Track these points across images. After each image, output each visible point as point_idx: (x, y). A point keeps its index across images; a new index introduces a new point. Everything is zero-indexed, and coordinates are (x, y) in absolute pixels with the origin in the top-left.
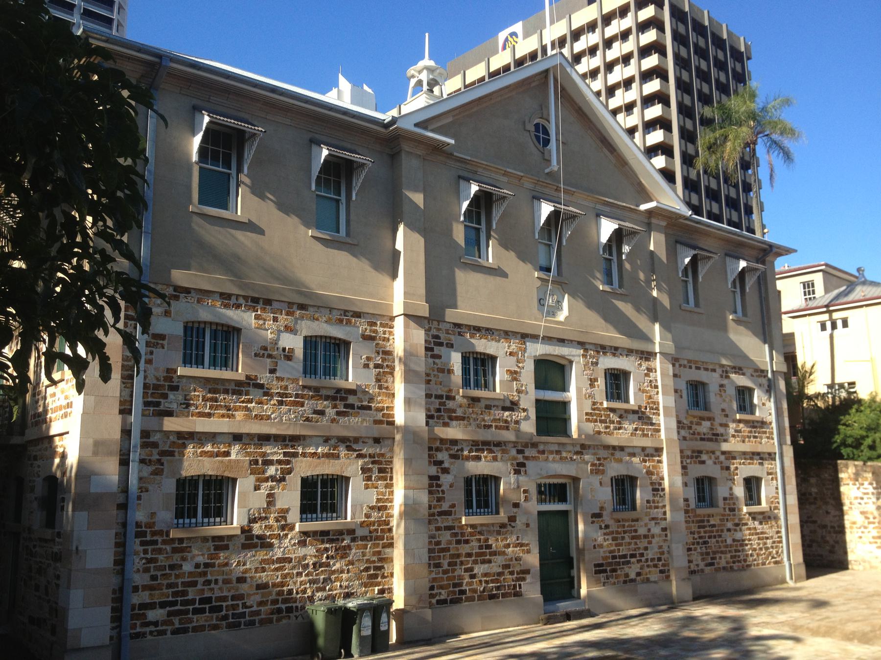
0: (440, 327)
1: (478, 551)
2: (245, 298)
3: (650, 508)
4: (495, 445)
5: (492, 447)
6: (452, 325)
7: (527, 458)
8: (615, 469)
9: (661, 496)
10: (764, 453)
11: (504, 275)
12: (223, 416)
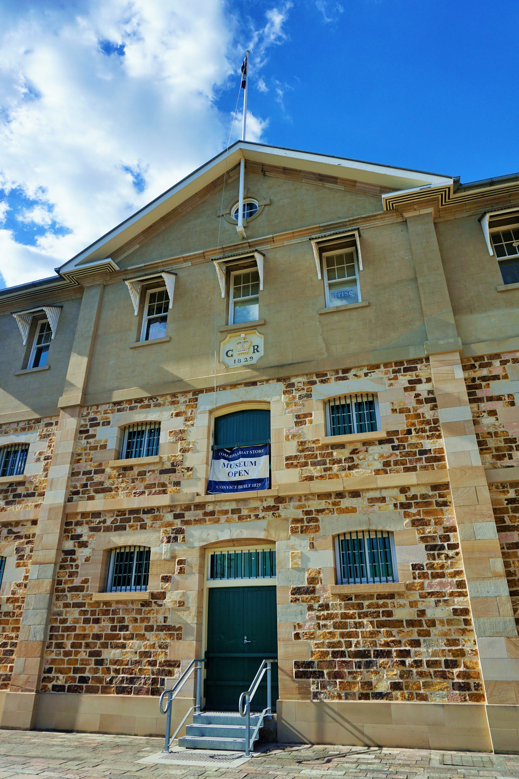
1: (110, 632)
3: (424, 576)
4: (145, 512)
5: (142, 516)
9: (447, 557)
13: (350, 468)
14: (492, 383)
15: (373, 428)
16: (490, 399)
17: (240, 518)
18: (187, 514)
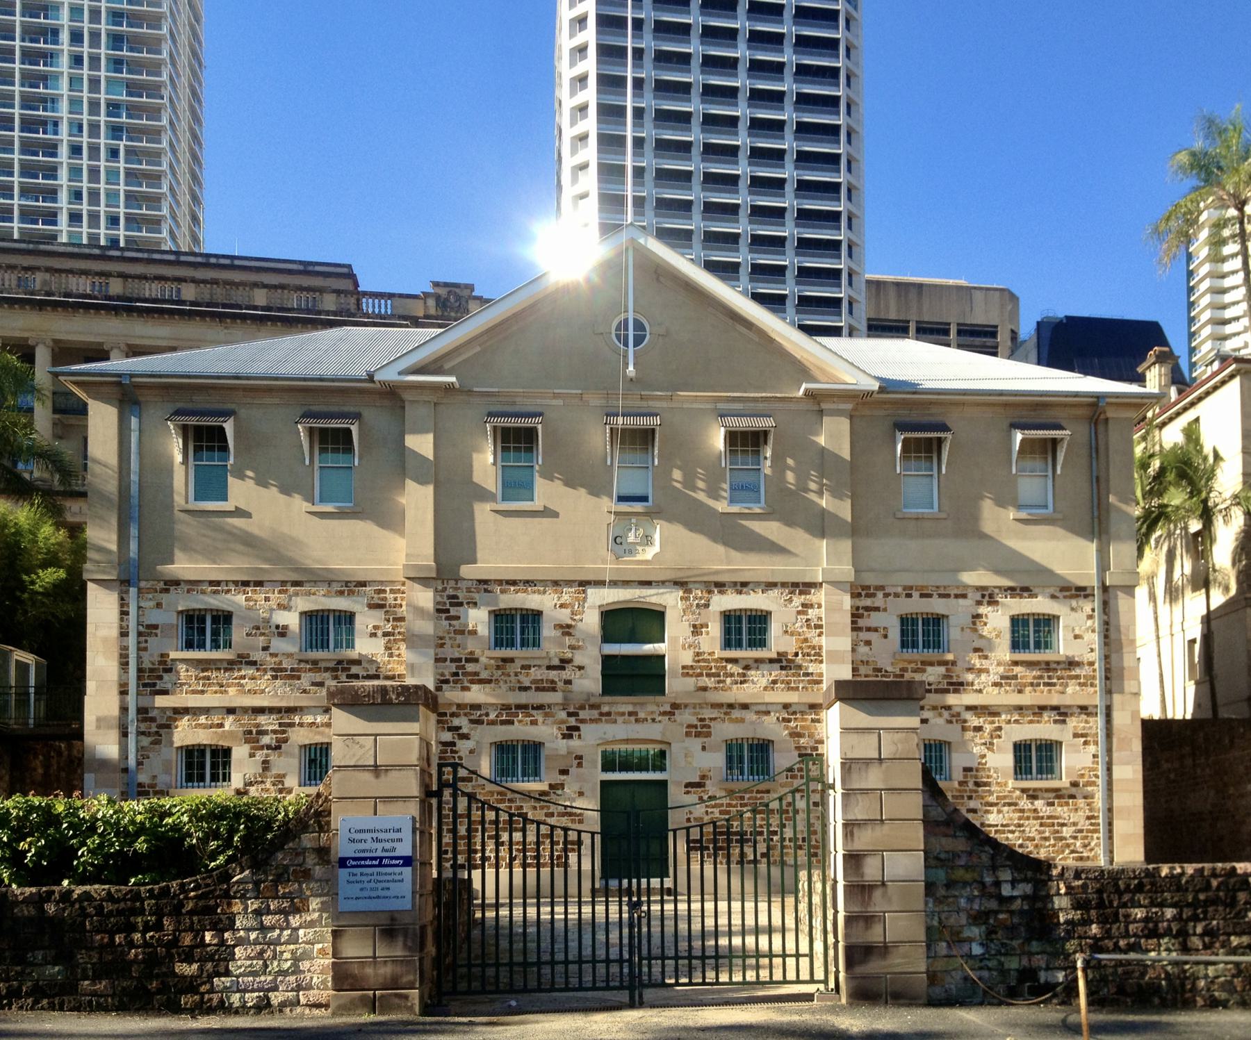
0: (459, 585)
2: (236, 583)
3: (793, 777)
4: (533, 708)
6: (475, 582)
7: (583, 721)
8: (727, 730)
10: (1069, 707)
11: (555, 515)
12: (216, 692)
13: (741, 683)
14: (872, 613)
15: (762, 643)
16: (869, 629)
17: (637, 721)
18: (581, 713)
